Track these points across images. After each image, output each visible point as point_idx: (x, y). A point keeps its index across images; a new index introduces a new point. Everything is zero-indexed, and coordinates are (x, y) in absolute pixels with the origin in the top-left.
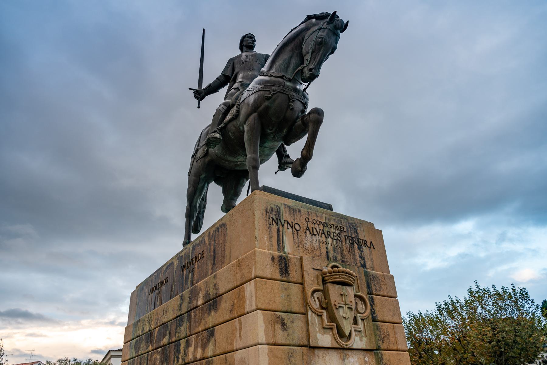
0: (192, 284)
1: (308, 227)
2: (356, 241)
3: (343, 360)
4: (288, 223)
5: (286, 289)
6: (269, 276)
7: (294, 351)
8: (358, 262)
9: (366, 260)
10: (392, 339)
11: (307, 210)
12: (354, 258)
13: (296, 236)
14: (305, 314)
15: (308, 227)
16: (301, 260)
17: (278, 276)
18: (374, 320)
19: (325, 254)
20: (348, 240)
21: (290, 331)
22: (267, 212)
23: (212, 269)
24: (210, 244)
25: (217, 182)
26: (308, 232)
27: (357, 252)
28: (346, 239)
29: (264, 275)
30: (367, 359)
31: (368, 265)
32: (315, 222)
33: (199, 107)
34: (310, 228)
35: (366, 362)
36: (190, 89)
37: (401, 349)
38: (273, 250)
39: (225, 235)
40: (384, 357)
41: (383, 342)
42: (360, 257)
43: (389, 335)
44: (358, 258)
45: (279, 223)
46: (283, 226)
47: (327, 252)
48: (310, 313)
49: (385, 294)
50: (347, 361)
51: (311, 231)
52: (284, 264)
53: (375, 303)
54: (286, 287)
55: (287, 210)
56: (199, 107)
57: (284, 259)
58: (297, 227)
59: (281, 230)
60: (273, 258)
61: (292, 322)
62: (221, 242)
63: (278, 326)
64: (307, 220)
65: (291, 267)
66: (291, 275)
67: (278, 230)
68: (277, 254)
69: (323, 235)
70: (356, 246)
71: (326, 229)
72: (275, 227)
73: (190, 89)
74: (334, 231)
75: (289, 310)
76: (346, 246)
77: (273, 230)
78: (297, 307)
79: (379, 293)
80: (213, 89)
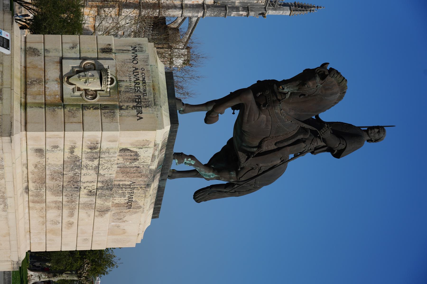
1: (138, 69)
2: (139, 105)
3: (56, 81)
4: (136, 56)
5: (93, 50)
6: (99, 42)
7: (59, 52)
8: (123, 104)
9: (126, 111)
10: (72, 119)
11: (150, 70)
12: (125, 101)
13: (129, 61)
14: (80, 58)
15: (138, 69)
16: (112, 59)
17: (100, 47)
18: (84, 107)
19: (122, 79)
20: (136, 97)
21: (69, 51)
22: (139, 44)
26: (134, 69)
27: (131, 104)
28: (138, 96)
29: (98, 40)
30: (57, 97)
31: (122, 111)
32: (143, 74)
34: (137, 71)
35: (56, 95)
37: (66, 125)
38: (115, 48)
40: (59, 110)
41: (69, 111)
42: (127, 106)
43: (74, 117)
44: (126, 104)
45: (134, 51)
46: (133, 53)
47: (124, 81)
48: (81, 61)
49: (103, 121)
50: (56, 83)
51: (135, 71)
52: (107, 50)
53: (95, 111)
54: (94, 50)
55: (146, 57)
57: (111, 51)
58: (135, 62)
59: (131, 52)
60: (110, 45)
61: (75, 53)
63: (72, 45)
64: (143, 69)
65: (107, 54)
66: (101, 54)
67: (129, 51)
69: (135, 79)
70: (135, 104)
71: (141, 82)
74: (141, 88)
75: (81, 52)
76: (132, 95)
77: (128, 47)
78: (82, 55)
79: (103, 116)
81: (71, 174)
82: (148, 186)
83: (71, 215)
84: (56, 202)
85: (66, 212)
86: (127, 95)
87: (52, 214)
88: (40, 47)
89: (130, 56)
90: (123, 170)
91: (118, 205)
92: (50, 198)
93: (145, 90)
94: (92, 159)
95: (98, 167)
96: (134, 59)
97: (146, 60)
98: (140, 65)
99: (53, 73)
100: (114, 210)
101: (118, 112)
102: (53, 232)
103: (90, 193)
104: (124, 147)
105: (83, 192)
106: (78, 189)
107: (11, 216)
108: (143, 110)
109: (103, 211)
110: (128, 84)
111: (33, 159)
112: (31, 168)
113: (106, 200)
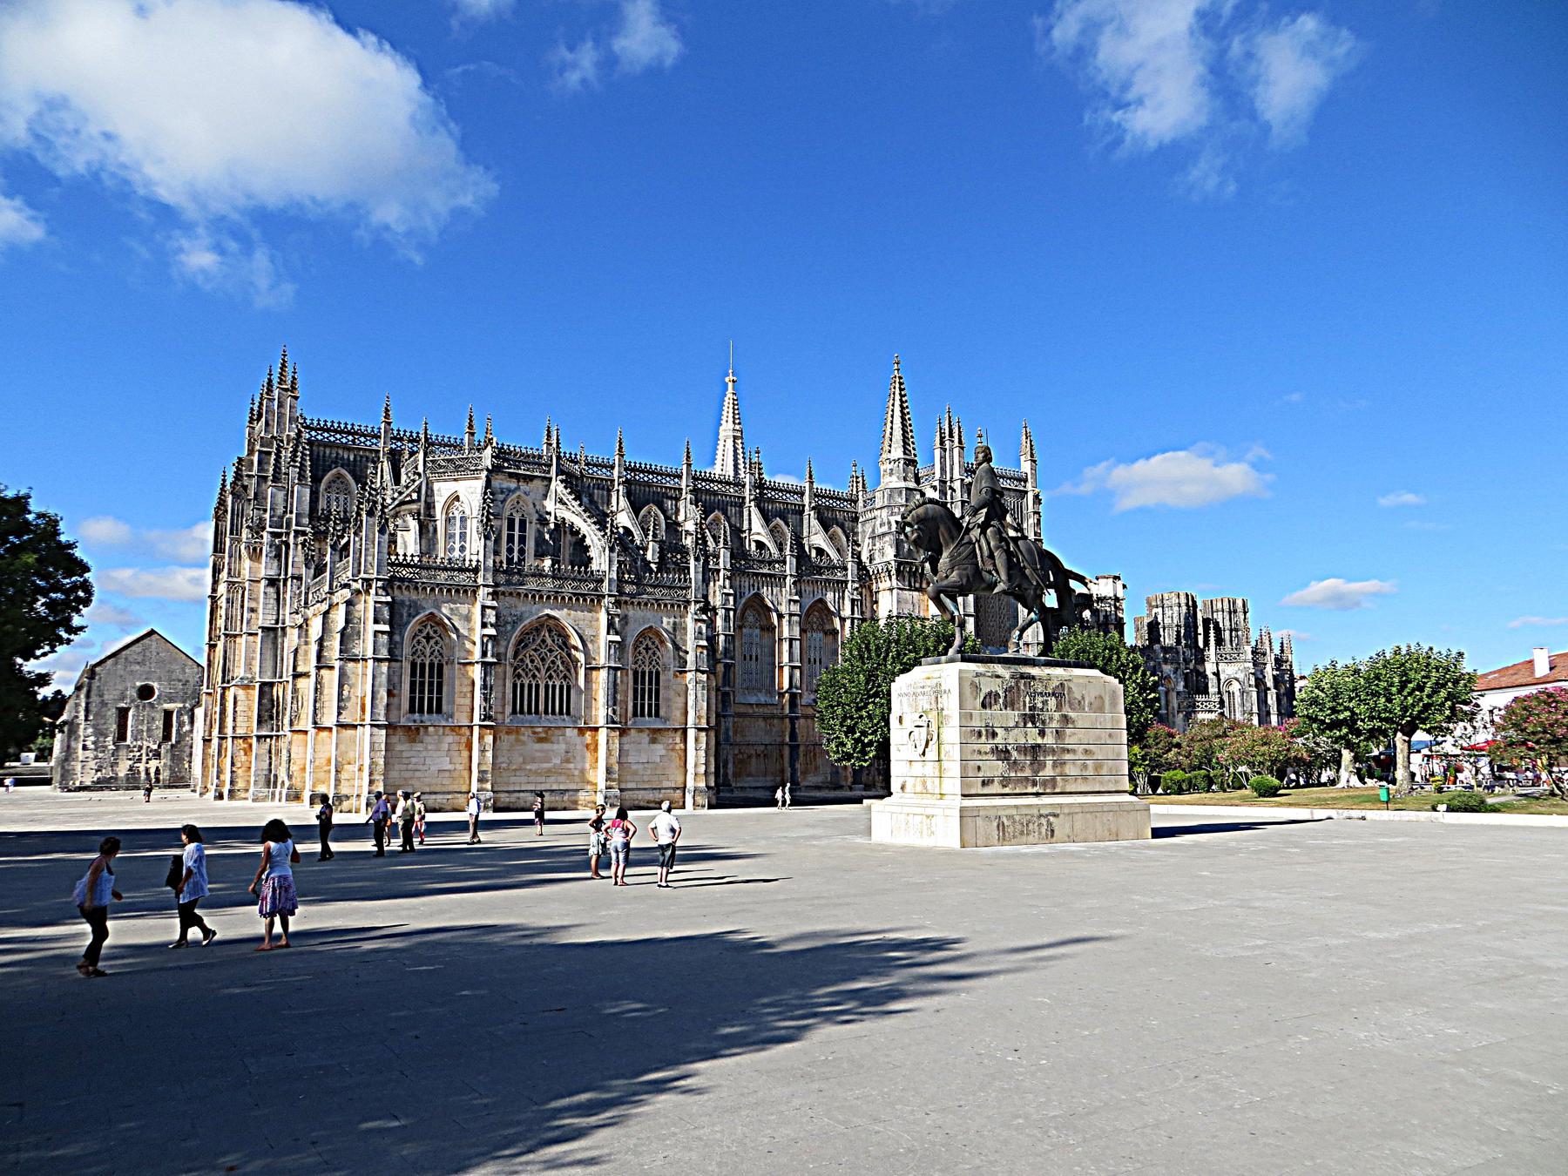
81: (1015, 754)
82: (1033, 678)
83: (1074, 751)
84: (1054, 766)
85: (1067, 757)
87: (1070, 770)
88: (901, 781)
89: (905, 699)
90: (1010, 704)
91: (1059, 707)
92: (1048, 771)
94: (994, 735)
95: (1006, 729)
98: (911, 691)
99: (917, 769)
100: (1066, 710)
102: (1097, 768)
103: (1042, 733)
104: (978, 705)
105: (1039, 741)
106: (1036, 748)
107: (1066, 811)
109: (1066, 719)
111: (996, 788)
112: (1007, 790)
113: (1051, 719)
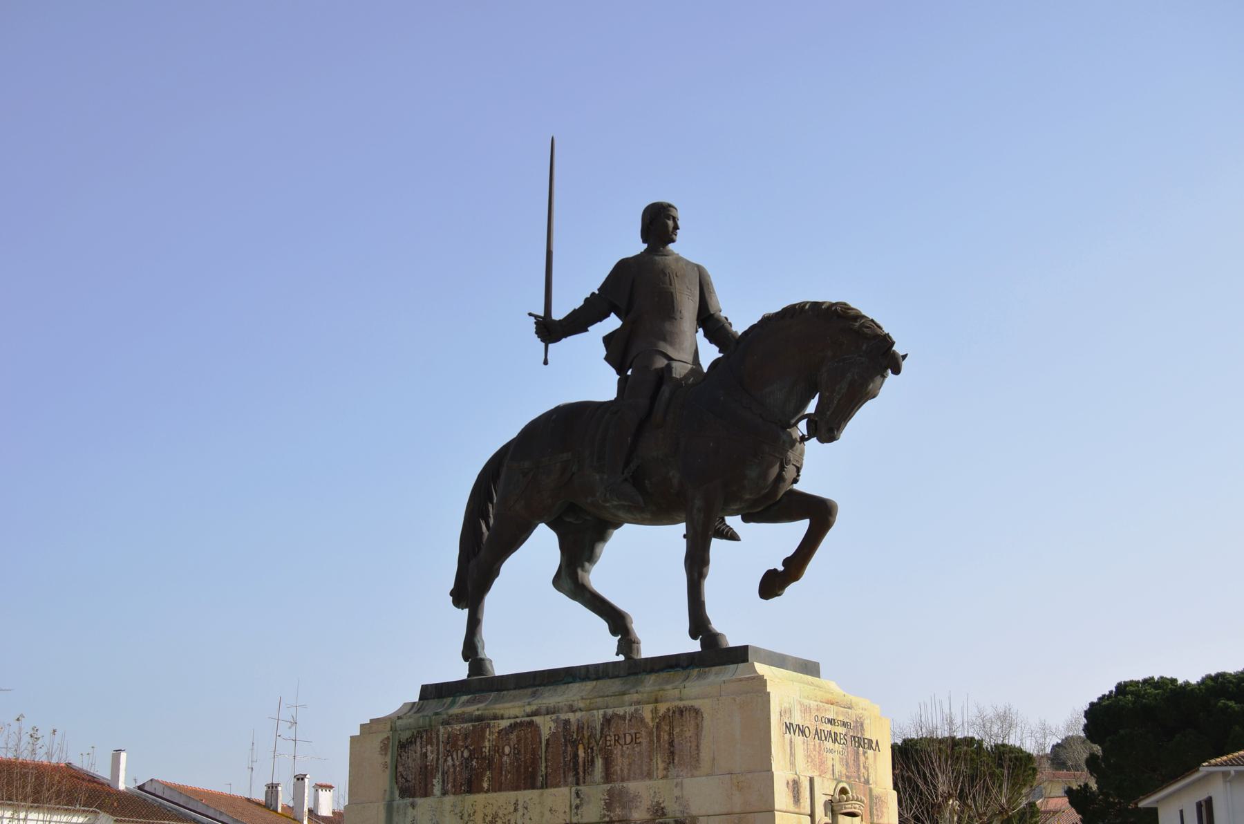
0: (608, 777)
16: (811, 780)
17: (792, 808)
23: (666, 769)
24: (658, 727)
25: (552, 525)
27: (862, 758)
33: (546, 363)
36: (530, 314)
39: (698, 728)
56: (546, 363)
62: (688, 734)
68: (791, 777)
72: (788, 736)
73: (530, 314)
80: (578, 322)
86: (851, 762)
89: (798, 739)
93: (844, 724)
96: (803, 732)
97: (806, 710)
101: (875, 792)
108: (867, 736)
110: (836, 756)
